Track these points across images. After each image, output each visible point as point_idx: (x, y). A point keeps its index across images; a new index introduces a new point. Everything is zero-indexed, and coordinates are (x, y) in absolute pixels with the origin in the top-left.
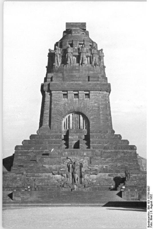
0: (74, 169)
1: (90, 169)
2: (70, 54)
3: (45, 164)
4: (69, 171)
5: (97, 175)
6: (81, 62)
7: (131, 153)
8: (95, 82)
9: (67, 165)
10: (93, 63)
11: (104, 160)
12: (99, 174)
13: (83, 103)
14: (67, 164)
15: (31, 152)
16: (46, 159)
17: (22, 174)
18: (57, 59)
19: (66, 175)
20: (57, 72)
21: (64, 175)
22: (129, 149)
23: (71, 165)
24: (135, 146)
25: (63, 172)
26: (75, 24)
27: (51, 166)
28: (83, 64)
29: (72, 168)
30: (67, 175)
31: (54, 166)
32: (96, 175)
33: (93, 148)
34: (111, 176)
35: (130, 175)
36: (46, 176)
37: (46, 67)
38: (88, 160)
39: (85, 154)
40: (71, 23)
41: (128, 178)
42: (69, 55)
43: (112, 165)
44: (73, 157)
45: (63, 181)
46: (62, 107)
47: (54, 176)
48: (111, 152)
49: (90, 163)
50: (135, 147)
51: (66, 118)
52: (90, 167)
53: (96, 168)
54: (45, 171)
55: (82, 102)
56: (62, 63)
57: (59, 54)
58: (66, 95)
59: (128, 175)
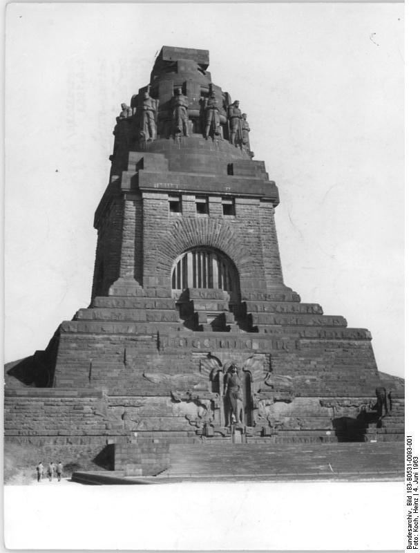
1: (272, 387)
2: (183, 110)
3: (152, 372)
5: (290, 404)
7: (360, 347)
8: (248, 178)
9: (211, 375)
11: (305, 363)
12: (297, 398)
13: (220, 225)
14: (209, 372)
15: (103, 339)
16: (158, 359)
17: (99, 395)
18: (149, 123)
19: (208, 403)
20: (151, 149)
21: (203, 402)
22: (356, 340)
23: (221, 375)
24: (367, 330)
25: (201, 394)
26: (184, 52)
27: (168, 376)
28: (215, 137)
29: (225, 383)
30: (213, 402)
31: (175, 377)
32: (289, 401)
33: (266, 331)
34: (326, 406)
35: (393, 400)
36: (155, 405)
38: (264, 363)
39: (255, 346)
40: (174, 48)
41: (388, 407)
42: (181, 112)
43: (327, 377)
44: (226, 353)
45: (203, 420)
46: (169, 232)
47: (176, 405)
48: (311, 343)
49: (271, 370)
51: (178, 262)
52: (270, 382)
53: (287, 384)
54: (151, 390)
55: (216, 226)
56: (158, 134)
58: (175, 207)
59: (388, 401)
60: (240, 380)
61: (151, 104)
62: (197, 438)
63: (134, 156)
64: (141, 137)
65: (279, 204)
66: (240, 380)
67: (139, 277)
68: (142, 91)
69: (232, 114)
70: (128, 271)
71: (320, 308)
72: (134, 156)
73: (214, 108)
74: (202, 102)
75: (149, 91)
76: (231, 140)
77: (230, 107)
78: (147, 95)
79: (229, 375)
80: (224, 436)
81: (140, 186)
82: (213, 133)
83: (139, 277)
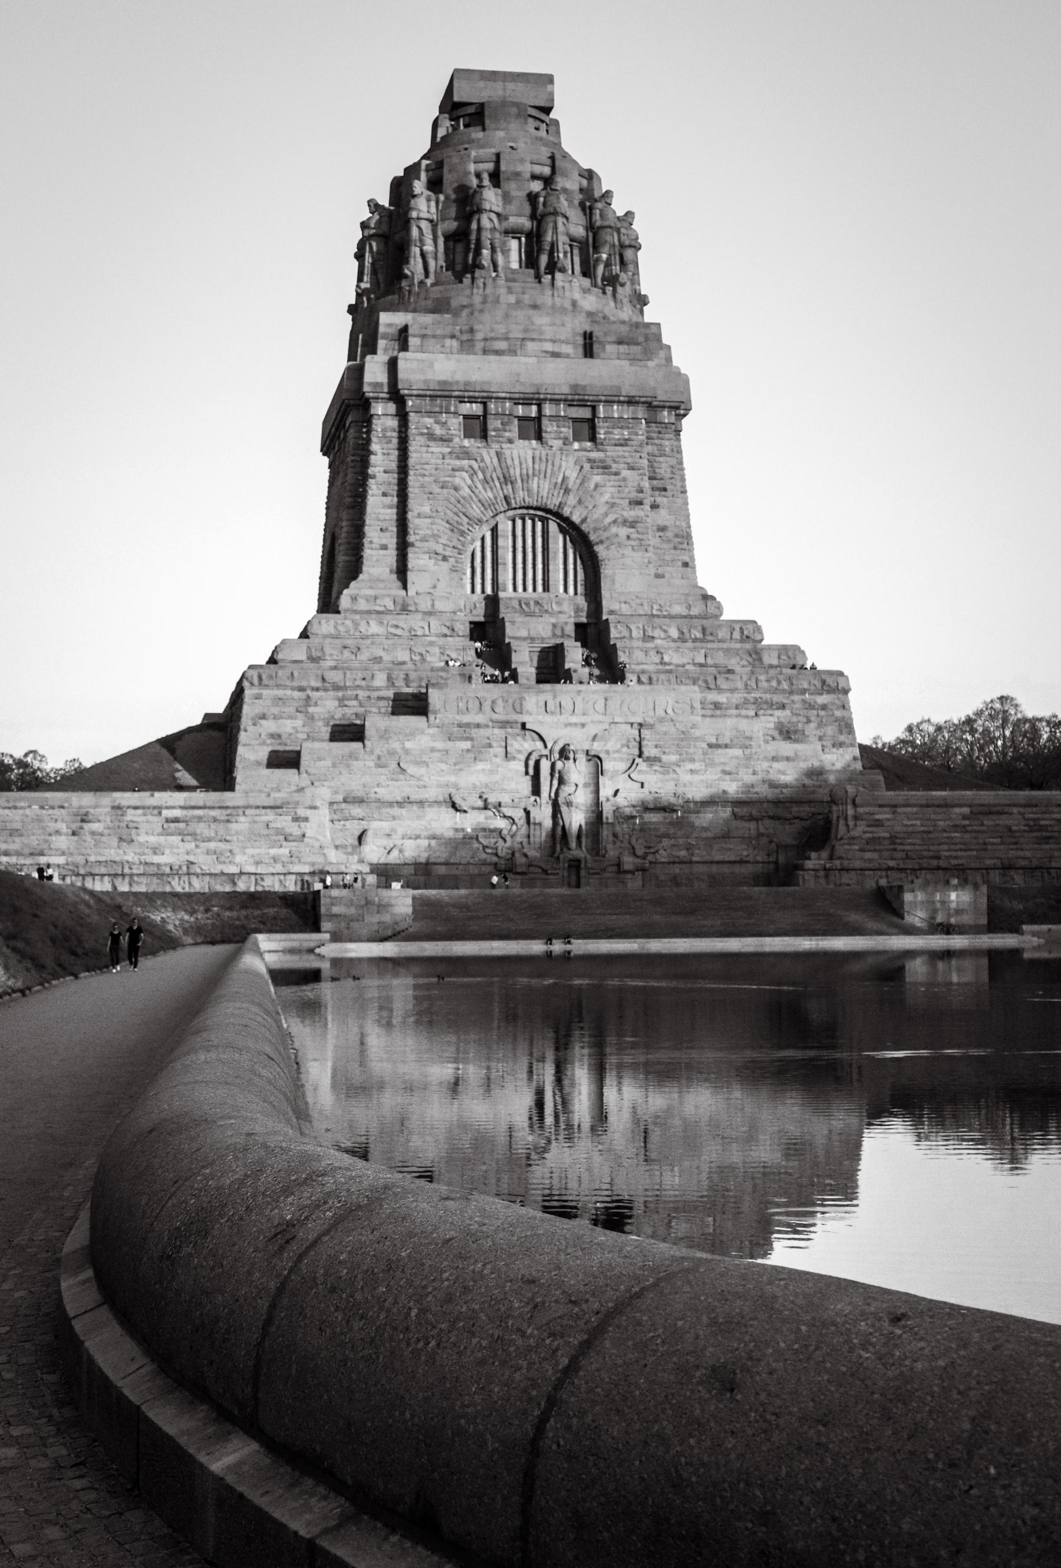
0: (561, 781)
4: (536, 791)
6: (544, 260)
24: (841, 674)
28: (558, 276)
29: (552, 775)
57: (431, 221)
60: (578, 772)
61: (424, 206)
63: (389, 320)
64: (406, 277)
65: (691, 412)
67: (402, 571)
68: (412, 171)
69: (598, 220)
70: (378, 559)
71: (758, 629)
72: (389, 320)
73: (555, 213)
74: (532, 198)
75: (423, 176)
76: (595, 278)
77: (592, 199)
78: (419, 186)
79: (559, 765)
80: (545, 872)
81: (400, 387)
82: (553, 267)
83: (402, 571)
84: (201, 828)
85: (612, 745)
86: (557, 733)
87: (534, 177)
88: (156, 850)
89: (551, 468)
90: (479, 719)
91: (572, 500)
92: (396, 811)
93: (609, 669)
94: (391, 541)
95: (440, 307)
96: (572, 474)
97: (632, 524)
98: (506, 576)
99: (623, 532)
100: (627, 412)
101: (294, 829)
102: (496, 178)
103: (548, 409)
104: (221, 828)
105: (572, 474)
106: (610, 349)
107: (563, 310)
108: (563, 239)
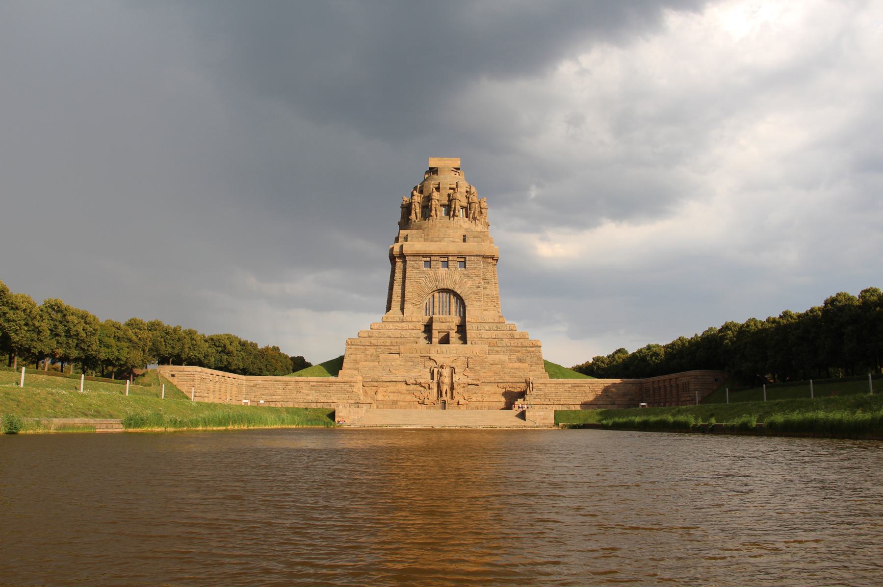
4: (432, 378)
10: (471, 215)
37: (399, 223)
42: (433, 202)
50: (539, 344)
62: (419, 406)
66: (446, 372)
67: (402, 309)
74: (449, 195)
82: (454, 215)
83: (402, 309)
84: (321, 388)
85: (459, 363)
86: (440, 359)
87: (451, 189)
88: (308, 395)
89: (451, 277)
90: (416, 355)
91: (457, 286)
92: (388, 384)
93: (464, 339)
94: (399, 299)
95: (419, 228)
96: (458, 278)
97: (477, 294)
98: (436, 311)
99: (474, 296)
100: (476, 259)
101: (350, 389)
102: (438, 189)
103: (450, 258)
104: (328, 389)
105: (458, 278)
106: (471, 239)
107: (457, 228)
108: (458, 207)
